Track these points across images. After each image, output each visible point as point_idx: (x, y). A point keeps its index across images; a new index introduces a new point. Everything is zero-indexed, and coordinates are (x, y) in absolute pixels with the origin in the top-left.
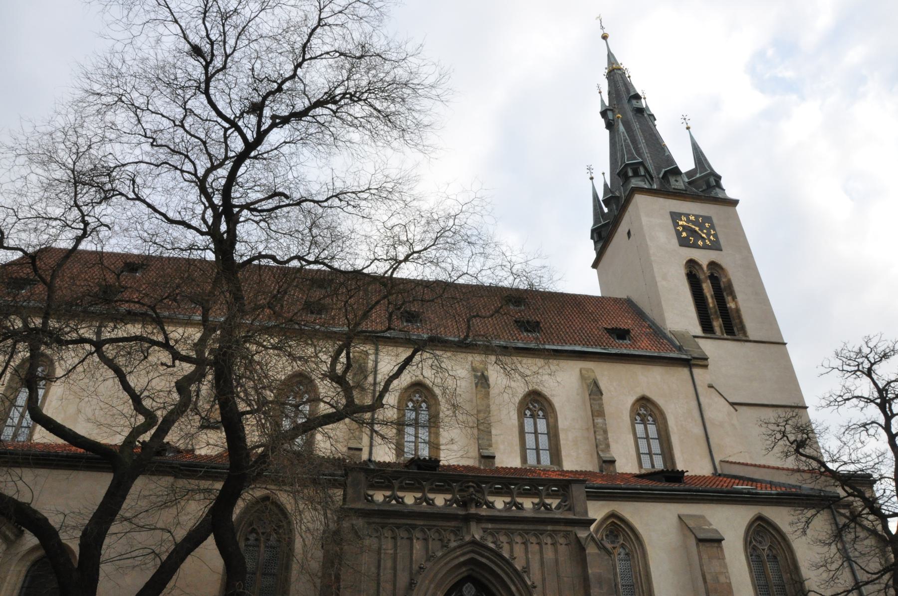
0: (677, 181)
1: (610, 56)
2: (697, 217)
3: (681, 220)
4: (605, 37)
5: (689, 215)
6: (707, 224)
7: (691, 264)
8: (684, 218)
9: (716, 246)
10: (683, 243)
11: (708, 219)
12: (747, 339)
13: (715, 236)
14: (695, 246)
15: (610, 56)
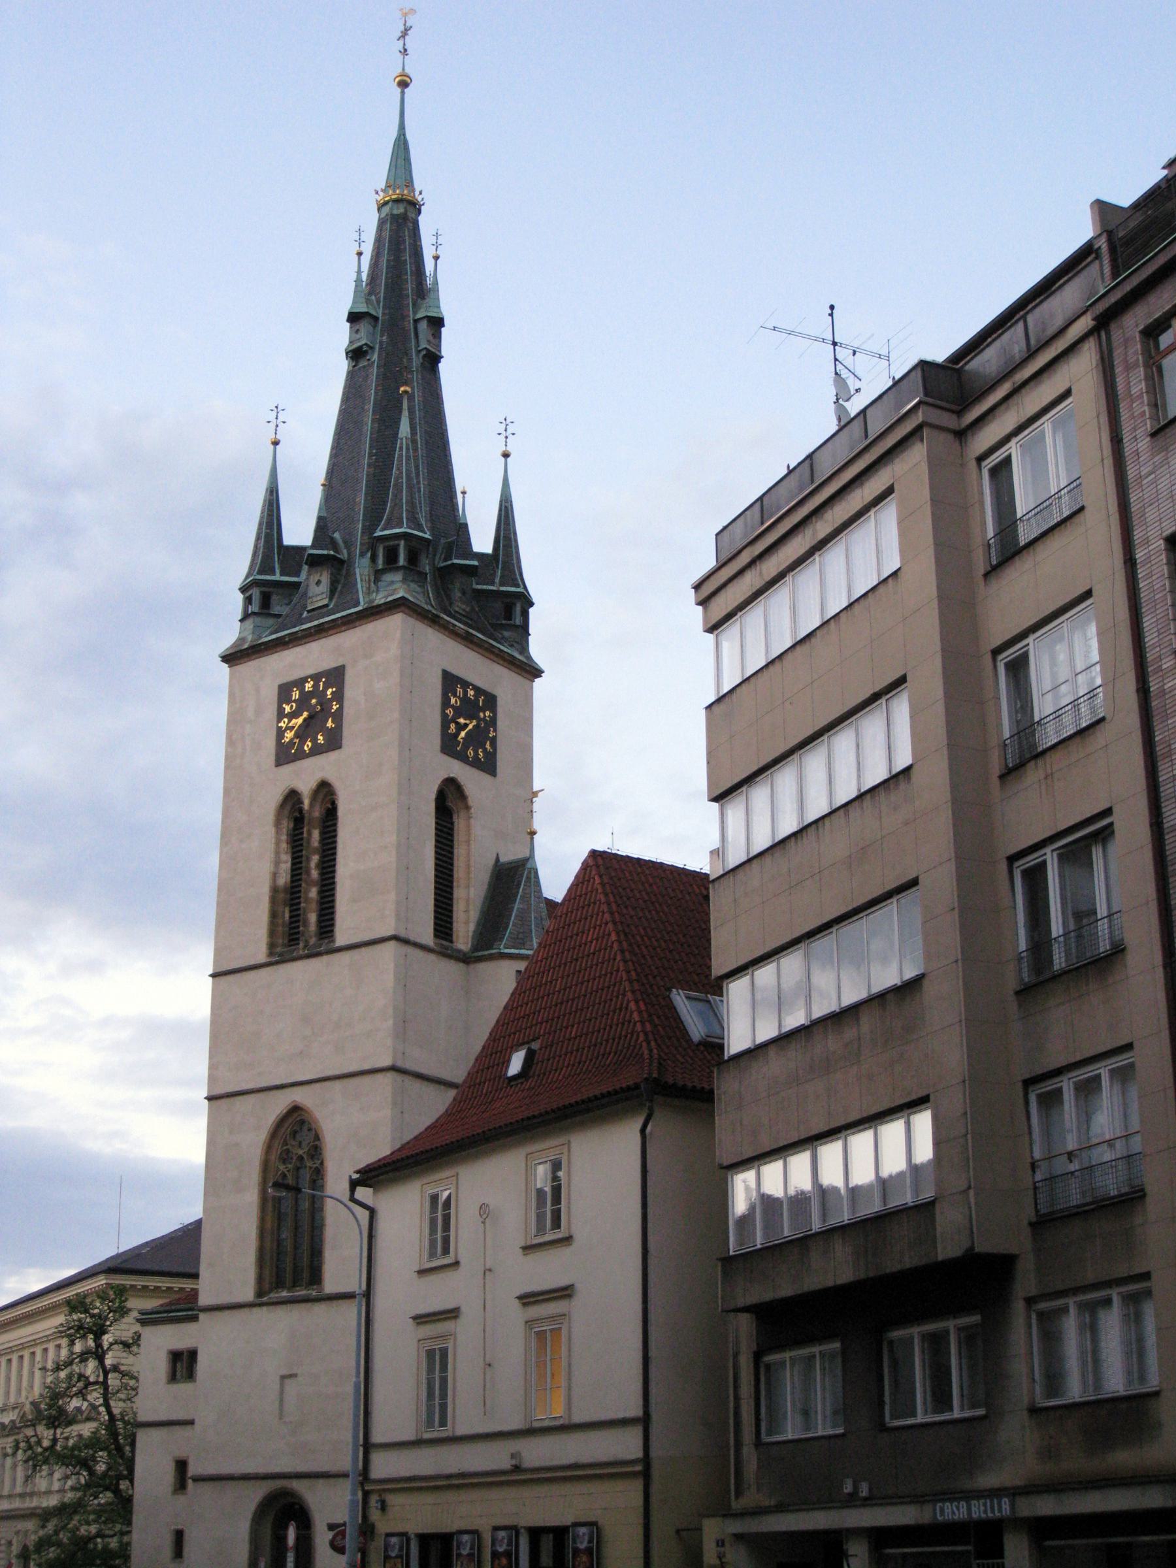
0: (318, 583)
1: (402, 148)
2: (316, 678)
3: (289, 702)
4: (404, 84)
5: (304, 680)
6: (329, 691)
7: (292, 796)
8: (296, 695)
9: (334, 742)
10: (285, 755)
11: (336, 676)
12: (331, 946)
13: (338, 717)
14: (301, 755)
15: (402, 148)
